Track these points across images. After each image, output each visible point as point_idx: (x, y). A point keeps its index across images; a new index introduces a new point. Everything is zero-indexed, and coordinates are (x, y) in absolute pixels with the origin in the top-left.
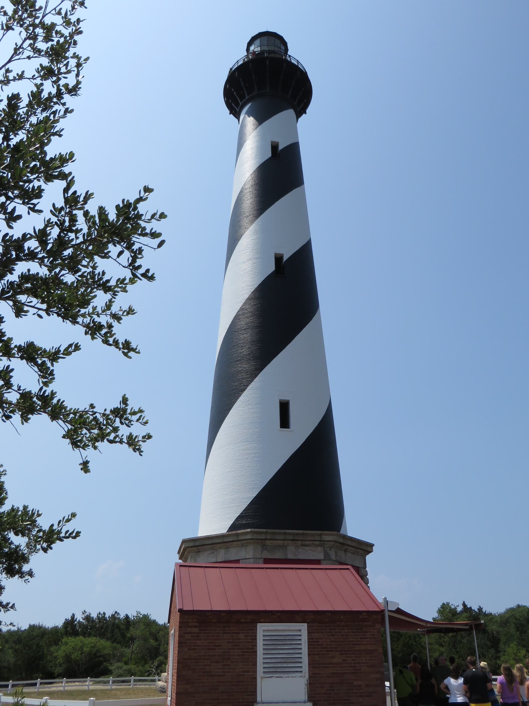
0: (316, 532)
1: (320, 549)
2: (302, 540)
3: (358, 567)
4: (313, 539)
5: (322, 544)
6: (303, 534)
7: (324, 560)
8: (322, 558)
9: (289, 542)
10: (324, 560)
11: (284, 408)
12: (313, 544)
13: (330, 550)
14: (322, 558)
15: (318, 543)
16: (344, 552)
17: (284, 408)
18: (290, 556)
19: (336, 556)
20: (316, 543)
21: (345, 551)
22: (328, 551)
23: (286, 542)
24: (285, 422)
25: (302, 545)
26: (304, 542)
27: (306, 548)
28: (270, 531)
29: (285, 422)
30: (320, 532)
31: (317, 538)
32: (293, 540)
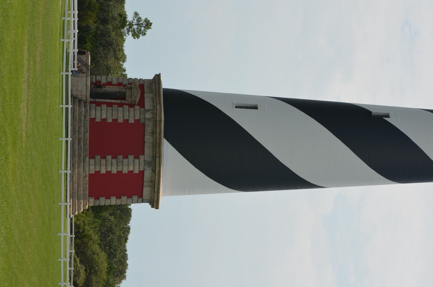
1: (152, 108)
16: (152, 131)
18: (146, 95)
19: (149, 119)
21: (153, 133)
27: (152, 102)
31: (157, 102)
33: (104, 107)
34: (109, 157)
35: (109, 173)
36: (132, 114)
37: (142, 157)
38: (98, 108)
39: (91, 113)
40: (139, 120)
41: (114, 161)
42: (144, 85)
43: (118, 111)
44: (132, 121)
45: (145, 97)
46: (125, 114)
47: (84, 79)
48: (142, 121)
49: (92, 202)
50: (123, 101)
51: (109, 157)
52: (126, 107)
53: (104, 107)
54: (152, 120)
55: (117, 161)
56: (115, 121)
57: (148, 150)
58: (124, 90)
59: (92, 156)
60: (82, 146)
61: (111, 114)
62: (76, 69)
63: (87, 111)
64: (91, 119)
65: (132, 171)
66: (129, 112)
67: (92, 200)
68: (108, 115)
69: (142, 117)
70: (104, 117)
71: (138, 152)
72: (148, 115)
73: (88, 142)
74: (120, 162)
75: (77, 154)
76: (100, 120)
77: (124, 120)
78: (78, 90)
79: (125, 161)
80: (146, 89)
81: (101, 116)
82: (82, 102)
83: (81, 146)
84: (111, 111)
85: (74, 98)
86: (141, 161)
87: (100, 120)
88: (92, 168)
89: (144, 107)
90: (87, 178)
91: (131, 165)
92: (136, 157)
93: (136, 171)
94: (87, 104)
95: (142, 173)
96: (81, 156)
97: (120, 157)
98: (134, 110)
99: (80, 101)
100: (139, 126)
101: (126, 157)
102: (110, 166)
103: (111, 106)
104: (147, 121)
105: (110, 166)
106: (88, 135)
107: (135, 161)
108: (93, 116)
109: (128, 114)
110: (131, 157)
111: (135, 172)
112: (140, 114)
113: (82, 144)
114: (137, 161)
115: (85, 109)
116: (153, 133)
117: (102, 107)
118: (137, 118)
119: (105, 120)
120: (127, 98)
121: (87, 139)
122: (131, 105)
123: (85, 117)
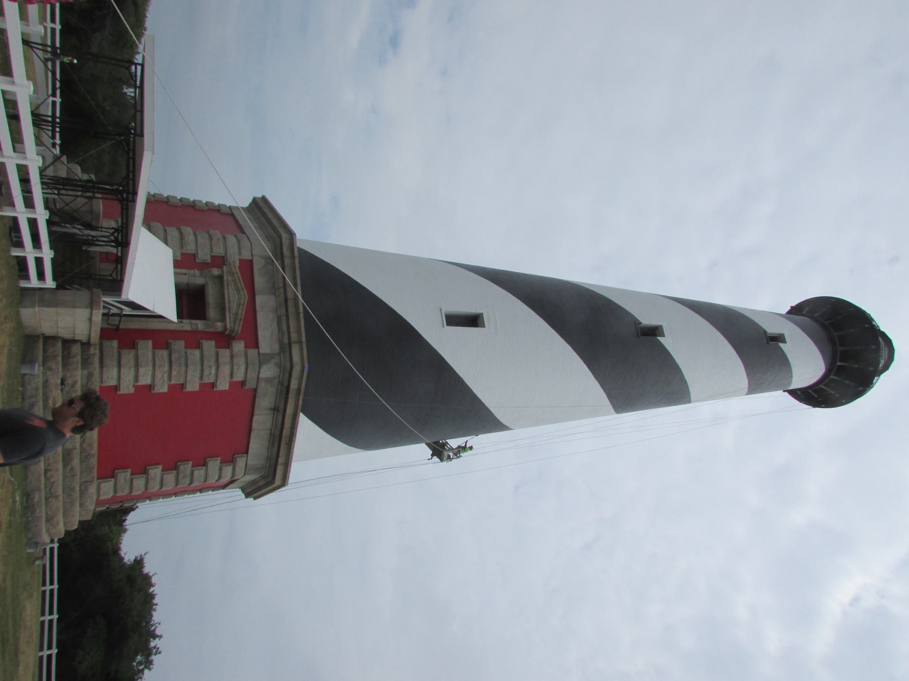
0: (303, 334)
1: (276, 347)
2: (287, 316)
3: (247, 453)
4: (292, 329)
5: (285, 348)
6: (298, 313)
7: (259, 353)
8: (262, 351)
9: (282, 295)
10: (259, 353)
11: (474, 321)
12: (283, 334)
13: (276, 364)
14: (262, 351)
15: (286, 341)
16: (272, 406)
17: (474, 321)
18: (259, 299)
19: (268, 381)
20: (286, 336)
21: (275, 409)
22: (273, 361)
23: (282, 290)
24: (454, 320)
25: (279, 319)
26: (284, 318)
27: (275, 325)
28: (297, 261)
29: (454, 320)
30: (304, 339)
31: (294, 336)
32: (286, 300)
33: (146, 347)
36: (225, 370)
37: (241, 462)
38: (128, 356)
39: (105, 376)
40: (243, 383)
42: (251, 261)
43: (187, 366)
44: (223, 385)
45: (258, 308)
46: (206, 372)
50: (200, 325)
52: (209, 346)
53: (146, 347)
54: (276, 381)
55: (178, 474)
56: (177, 389)
57: (258, 445)
58: (200, 281)
60: (78, 470)
61: (166, 376)
62: (50, 283)
63: (90, 375)
66: (218, 367)
68: (159, 375)
69: (252, 375)
70: (145, 380)
72: (268, 371)
73: (95, 451)
74: (184, 477)
75: (60, 491)
76: (132, 390)
77: (202, 386)
78: (60, 325)
80: (259, 281)
81: (136, 378)
82: (76, 349)
83: (72, 468)
84: (166, 368)
86: (237, 469)
87: (132, 390)
89: (256, 346)
92: (230, 460)
94: (92, 350)
96: (73, 489)
98: (232, 357)
99: (68, 343)
100: (243, 397)
101: (202, 463)
103: (167, 346)
104: (262, 385)
107: (224, 471)
108: (113, 383)
109: (213, 371)
112: (247, 369)
113: (76, 462)
115: (85, 372)
116: (278, 410)
117: (140, 352)
118: (239, 377)
119: (150, 387)
120: (212, 313)
121: (91, 445)
122: (224, 340)
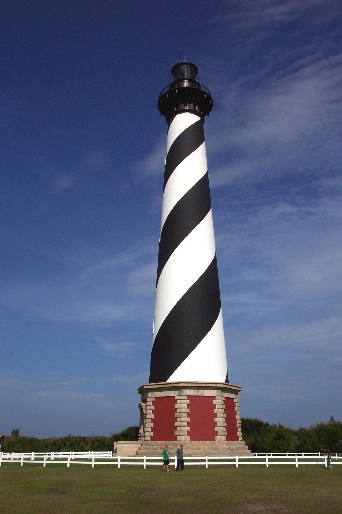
19: (152, 395)
34: (176, 424)
35: (189, 424)
37: (176, 398)
41: (178, 419)
47: (119, 446)
48: (154, 399)
49: (221, 437)
51: (176, 424)
57: (172, 393)
59: (175, 438)
64: (151, 440)
65: (188, 405)
67: (218, 437)
71: (172, 400)
76: (152, 433)
79: (178, 411)
85: (137, 454)
88: (183, 438)
90: (193, 442)
91: (183, 406)
93: (188, 401)
95: (189, 397)
97: (176, 415)
102: (183, 423)
105: (183, 423)
106: (159, 442)
110: (176, 406)
111: (189, 403)
114: (178, 401)
123: (148, 444)
